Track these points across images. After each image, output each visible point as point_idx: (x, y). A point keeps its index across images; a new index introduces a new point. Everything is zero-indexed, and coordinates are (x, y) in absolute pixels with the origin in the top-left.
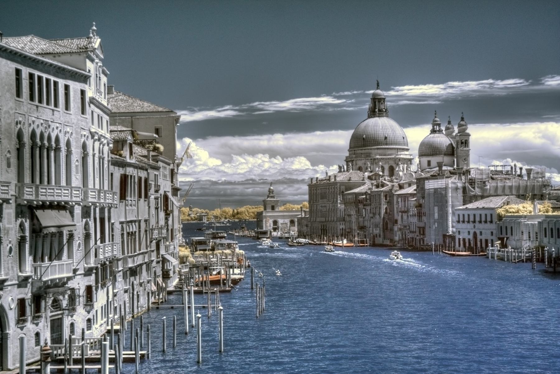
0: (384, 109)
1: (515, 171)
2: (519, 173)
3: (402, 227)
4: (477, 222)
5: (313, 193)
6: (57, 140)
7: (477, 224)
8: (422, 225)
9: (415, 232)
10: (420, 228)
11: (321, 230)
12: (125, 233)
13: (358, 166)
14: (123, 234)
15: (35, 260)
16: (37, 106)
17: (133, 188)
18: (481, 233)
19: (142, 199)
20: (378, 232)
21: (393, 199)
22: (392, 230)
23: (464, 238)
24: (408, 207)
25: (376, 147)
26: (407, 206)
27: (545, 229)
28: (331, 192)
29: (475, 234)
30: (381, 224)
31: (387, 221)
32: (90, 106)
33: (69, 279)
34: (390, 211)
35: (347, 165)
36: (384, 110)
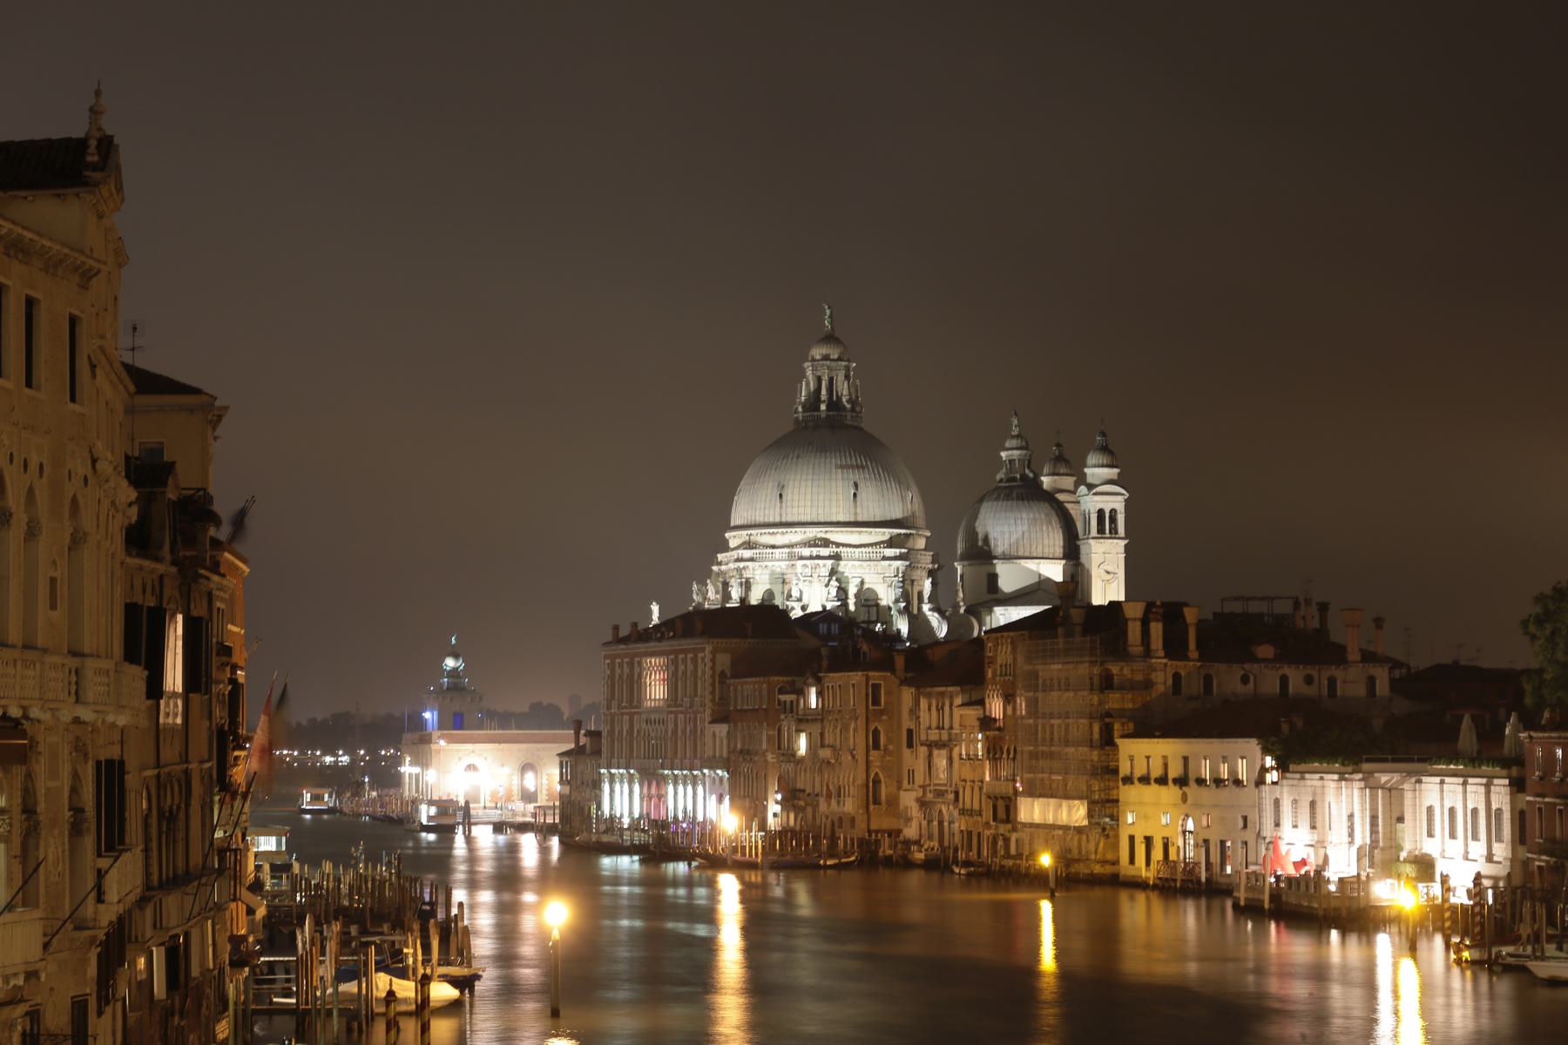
2: (1315, 624)
3: (930, 796)
5: (621, 677)
8: (1004, 788)
9: (981, 815)
10: (994, 798)
12: (154, 813)
22: (893, 802)
23: (1148, 835)
24: (951, 728)
26: (947, 726)
27: (1430, 809)
28: (685, 673)
31: (876, 773)
32: (94, 375)
34: (890, 741)
36: (848, 406)
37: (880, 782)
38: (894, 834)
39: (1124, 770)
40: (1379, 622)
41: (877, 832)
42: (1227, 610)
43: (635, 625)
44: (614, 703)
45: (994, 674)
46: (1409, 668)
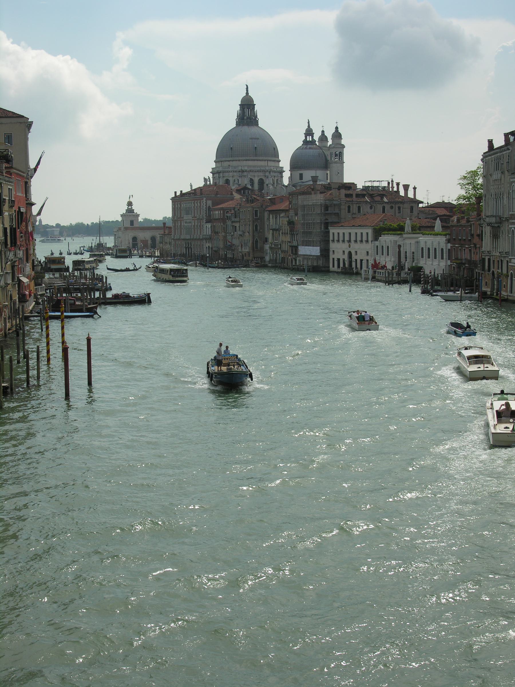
0: (254, 116)
1: (393, 187)
2: (395, 189)
3: (273, 246)
4: (352, 241)
5: (177, 208)
8: (295, 243)
11: (186, 248)
13: (225, 179)
18: (356, 252)
20: (247, 250)
21: (264, 216)
22: (262, 249)
23: (339, 258)
25: (244, 158)
26: (278, 224)
27: (422, 248)
28: (197, 207)
29: (350, 253)
30: (251, 242)
35: (213, 178)
37: (258, 241)
38: (262, 258)
39: (331, 238)
40: (415, 188)
41: (256, 258)
42: (366, 185)
43: (181, 191)
44: (176, 217)
45: (292, 206)
46: (428, 203)
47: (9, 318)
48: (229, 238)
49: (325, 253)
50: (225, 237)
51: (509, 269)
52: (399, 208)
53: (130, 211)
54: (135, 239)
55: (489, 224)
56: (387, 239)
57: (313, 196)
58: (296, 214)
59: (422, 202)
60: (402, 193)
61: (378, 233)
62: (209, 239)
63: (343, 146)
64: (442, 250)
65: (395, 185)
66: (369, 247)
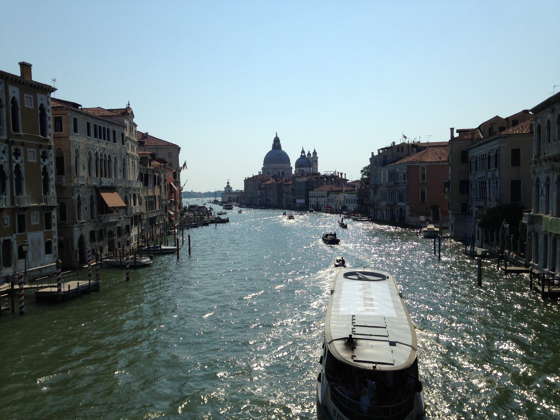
1: (336, 174)
2: (337, 175)
6: (109, 156)
7: (319, 198)
8: (294, 198)
14: (146, 202)
15: (99, 213)
16: (99, 141)
17: (151, 180)
19: (156, 186)
29: (317, 202)
33: (117, 222)
35: (262, 171)
39: (309, 196)
40: (345, 174)
47: (163, 229)
48: (268, 196)
49: (307, 202)
50: (266, 196)
51: (381, 206)
52: (339, 183)
53: (228, 186)
54: (230, 198)
55: (372, 188)
56: (332, 196)
57: (302, 178)
58: (295, 186)
59: (348, 180)
60: (340, 177)
61: (329, 193)
62: (260, 197)
63: (318, 158)
64: (355, 200)
65: (337, 173)
66: (325, 199)
